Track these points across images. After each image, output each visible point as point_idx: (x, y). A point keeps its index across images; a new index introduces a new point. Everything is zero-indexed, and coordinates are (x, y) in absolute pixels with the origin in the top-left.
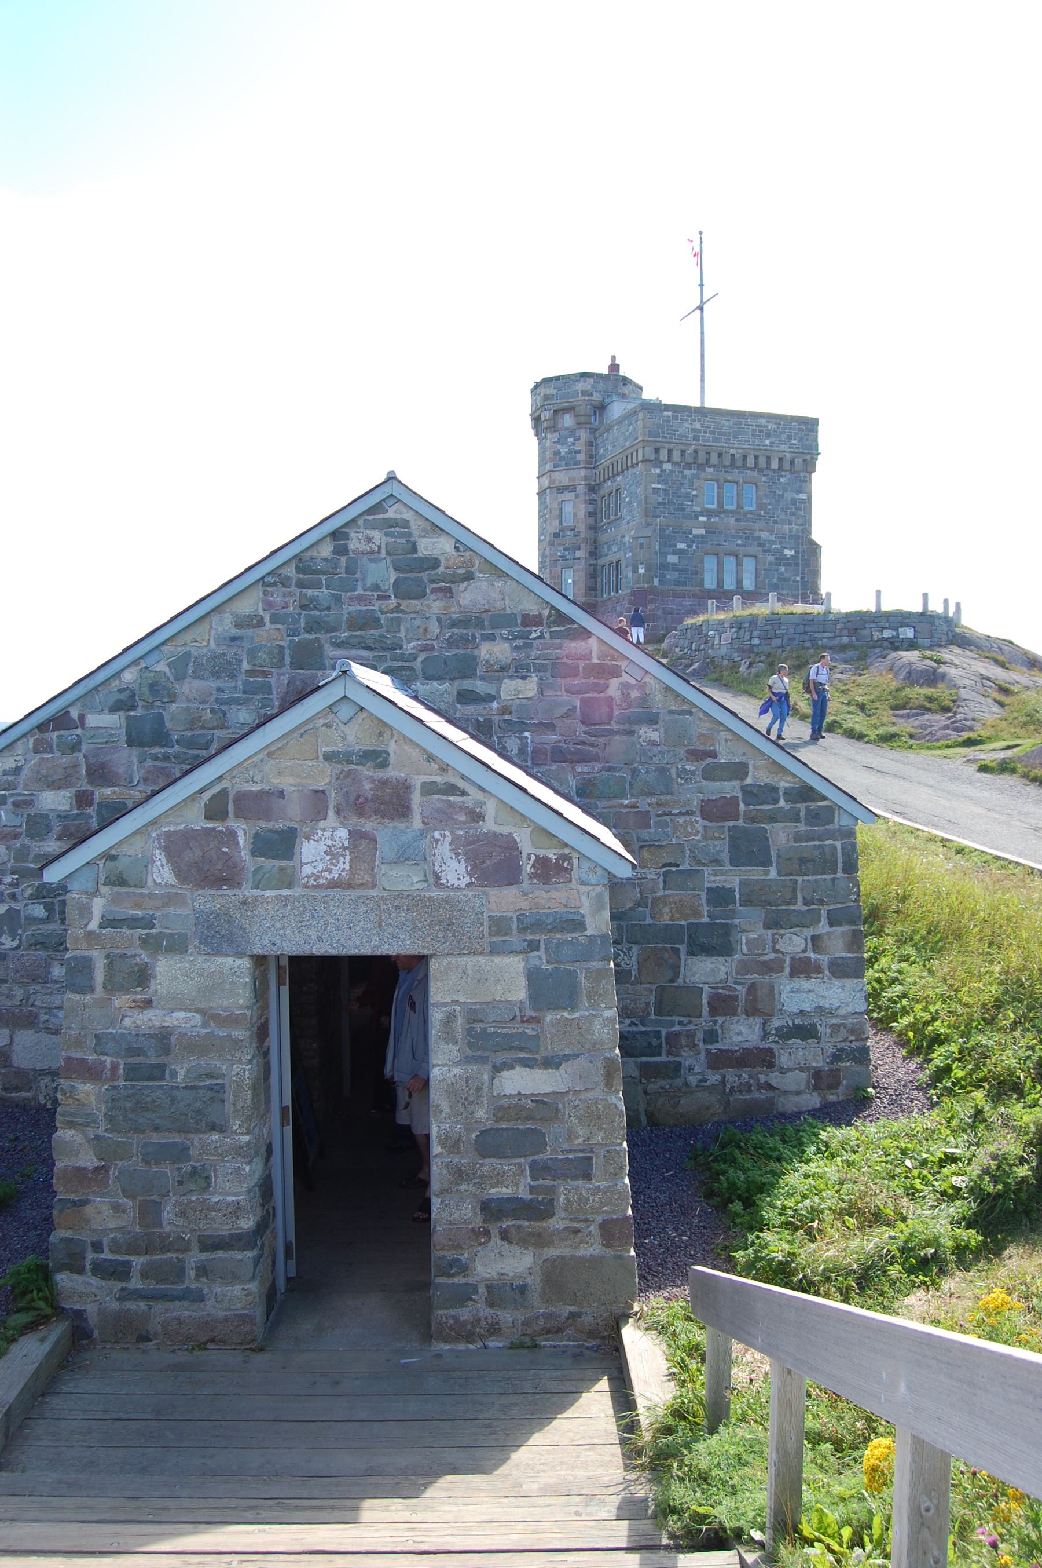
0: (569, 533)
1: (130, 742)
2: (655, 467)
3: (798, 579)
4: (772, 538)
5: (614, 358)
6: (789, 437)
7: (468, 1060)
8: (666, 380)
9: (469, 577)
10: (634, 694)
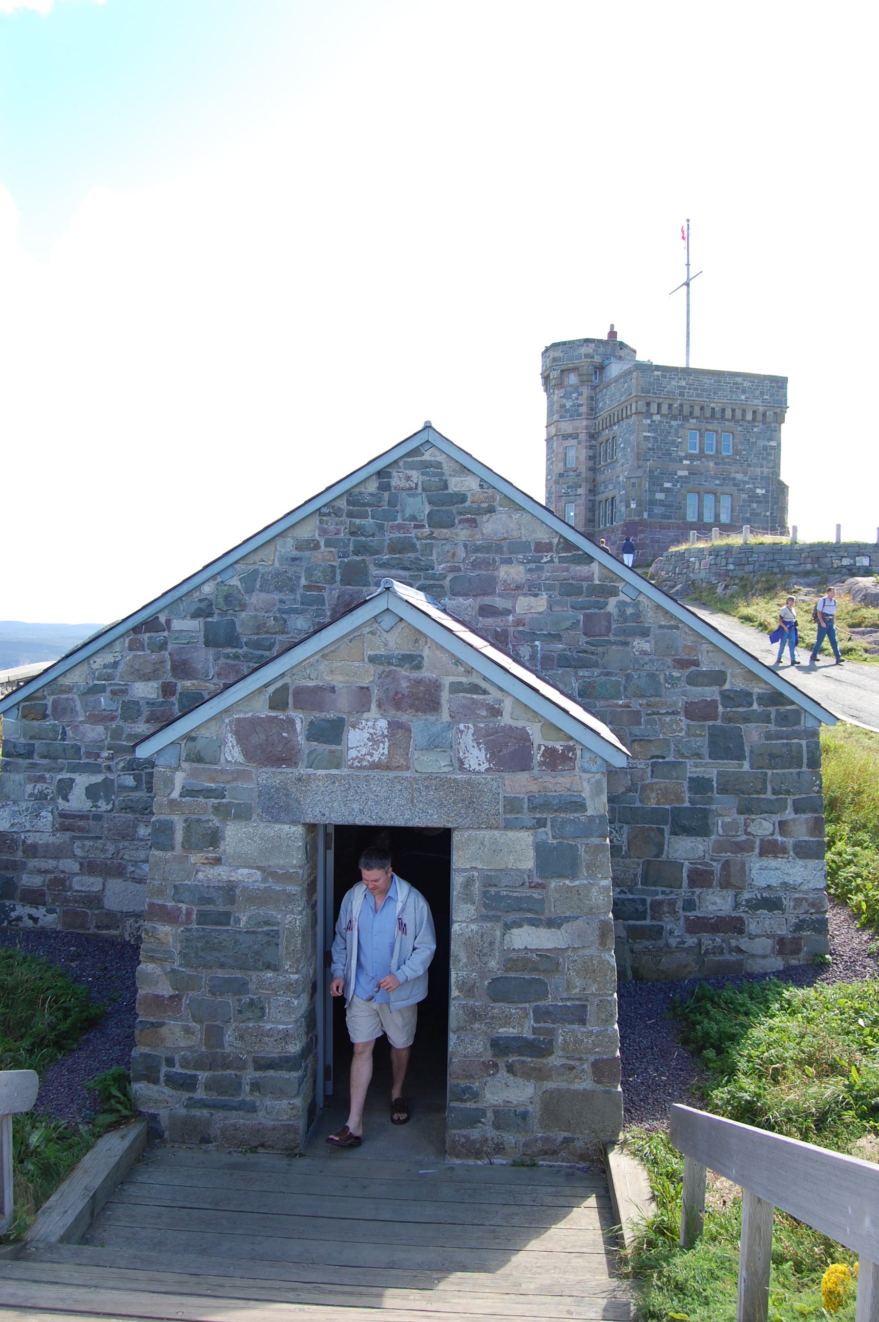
0: (572, 473)
1: (207, 644)
2: (646, 418)
3: (768, 514)
4: (746, 479)
5: (612, 326)
6: (762, 393)
7: (484, 918)
8: (656, 344)
9: (491, 510)
10: (630, 611)
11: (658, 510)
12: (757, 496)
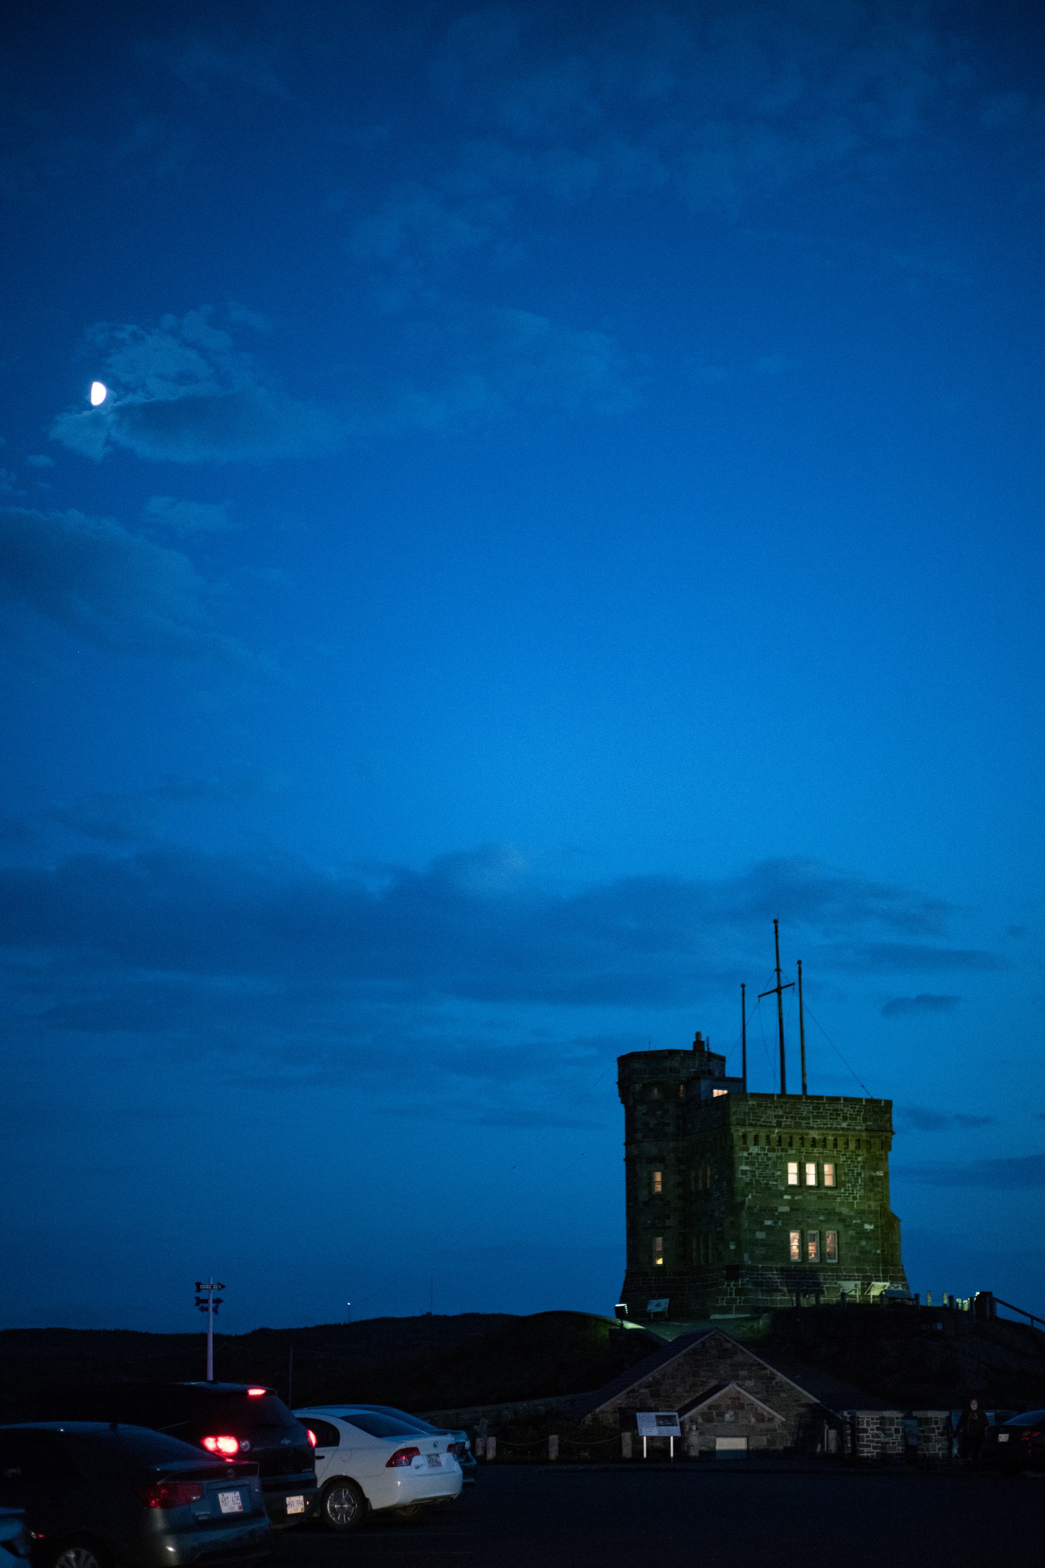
3: (879, 1251)
4: (852, 1213)
5: (698, 1035)
11: (760, 1251)
12: (865, 1232)
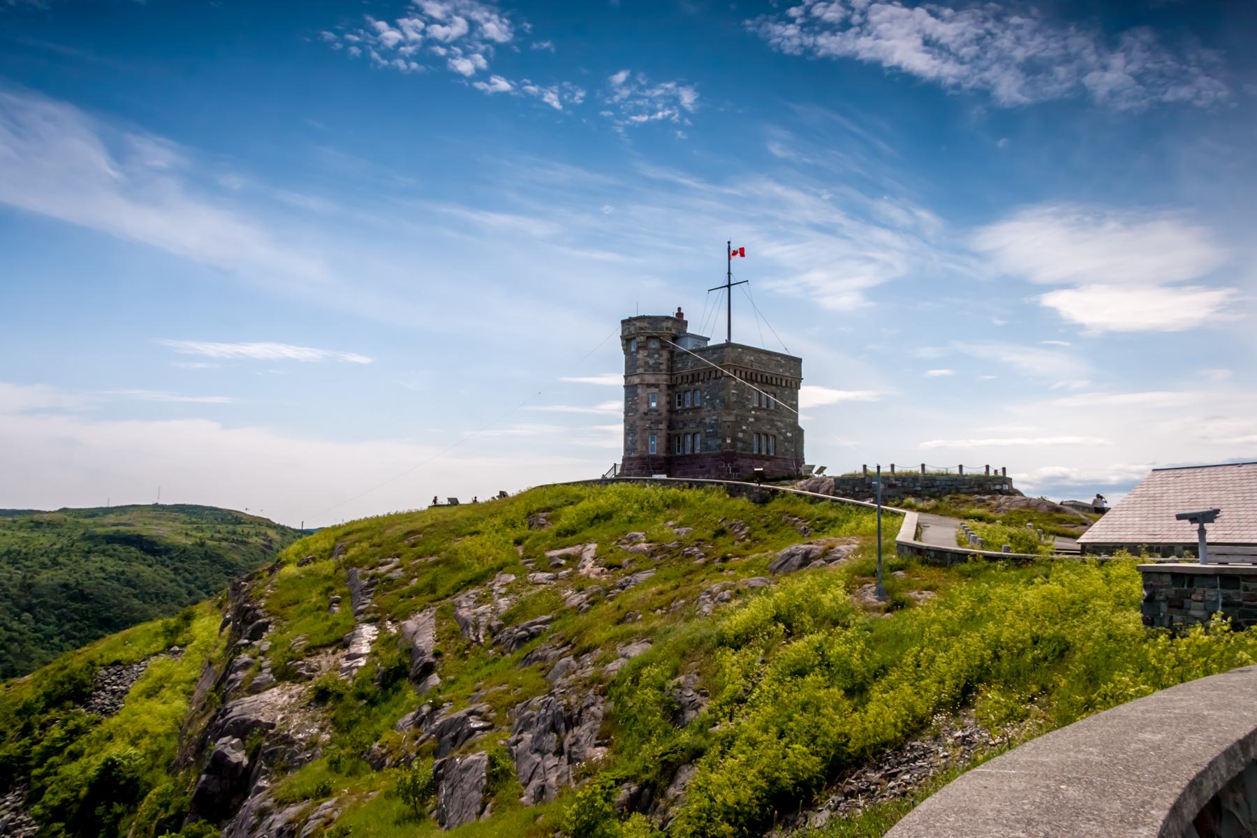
8: (708, 324)
